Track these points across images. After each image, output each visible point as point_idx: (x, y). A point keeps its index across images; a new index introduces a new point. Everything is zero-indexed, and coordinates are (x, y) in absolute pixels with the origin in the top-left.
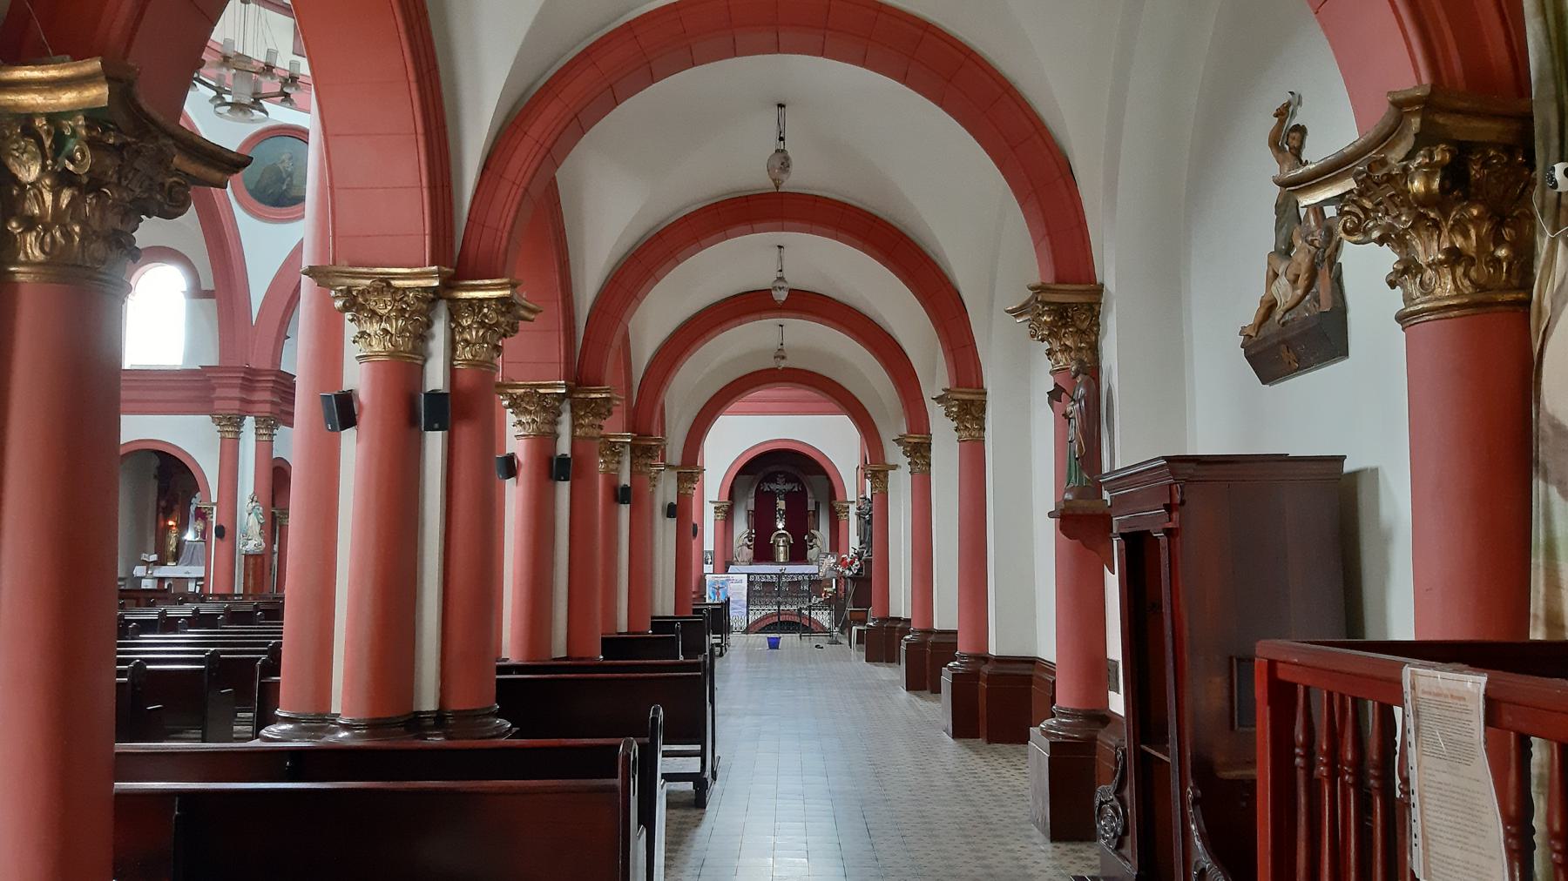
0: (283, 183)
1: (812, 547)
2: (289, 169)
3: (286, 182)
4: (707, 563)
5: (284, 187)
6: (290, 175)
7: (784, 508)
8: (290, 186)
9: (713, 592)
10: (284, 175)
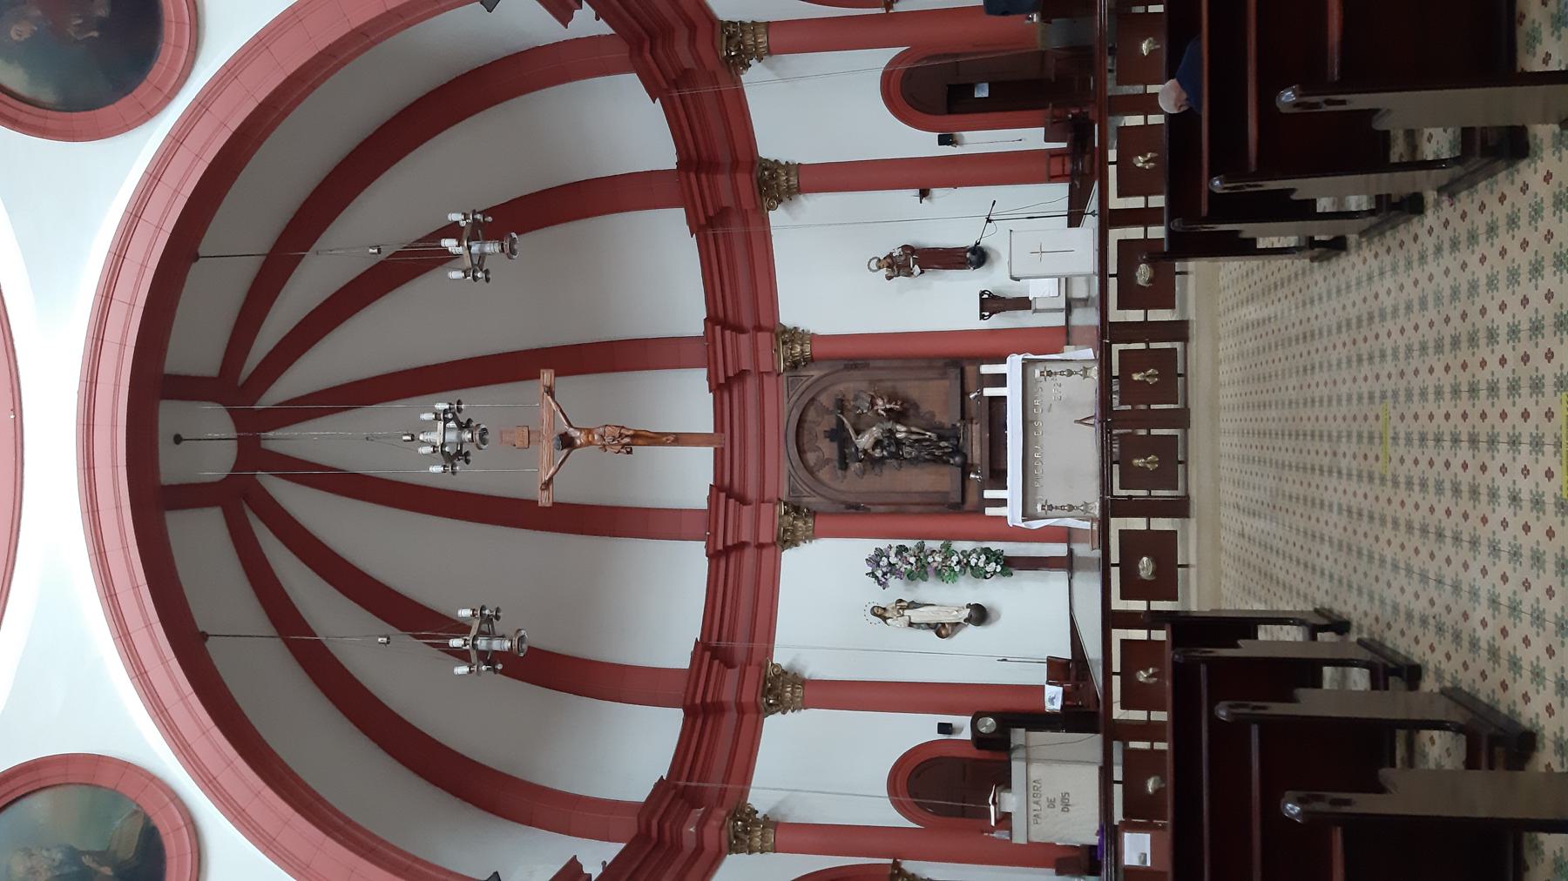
0: (96, 873)
2: (59, 856)
3: (94, 865)
5: (107, 871)
6: (74, 855)
8: (101, 856)
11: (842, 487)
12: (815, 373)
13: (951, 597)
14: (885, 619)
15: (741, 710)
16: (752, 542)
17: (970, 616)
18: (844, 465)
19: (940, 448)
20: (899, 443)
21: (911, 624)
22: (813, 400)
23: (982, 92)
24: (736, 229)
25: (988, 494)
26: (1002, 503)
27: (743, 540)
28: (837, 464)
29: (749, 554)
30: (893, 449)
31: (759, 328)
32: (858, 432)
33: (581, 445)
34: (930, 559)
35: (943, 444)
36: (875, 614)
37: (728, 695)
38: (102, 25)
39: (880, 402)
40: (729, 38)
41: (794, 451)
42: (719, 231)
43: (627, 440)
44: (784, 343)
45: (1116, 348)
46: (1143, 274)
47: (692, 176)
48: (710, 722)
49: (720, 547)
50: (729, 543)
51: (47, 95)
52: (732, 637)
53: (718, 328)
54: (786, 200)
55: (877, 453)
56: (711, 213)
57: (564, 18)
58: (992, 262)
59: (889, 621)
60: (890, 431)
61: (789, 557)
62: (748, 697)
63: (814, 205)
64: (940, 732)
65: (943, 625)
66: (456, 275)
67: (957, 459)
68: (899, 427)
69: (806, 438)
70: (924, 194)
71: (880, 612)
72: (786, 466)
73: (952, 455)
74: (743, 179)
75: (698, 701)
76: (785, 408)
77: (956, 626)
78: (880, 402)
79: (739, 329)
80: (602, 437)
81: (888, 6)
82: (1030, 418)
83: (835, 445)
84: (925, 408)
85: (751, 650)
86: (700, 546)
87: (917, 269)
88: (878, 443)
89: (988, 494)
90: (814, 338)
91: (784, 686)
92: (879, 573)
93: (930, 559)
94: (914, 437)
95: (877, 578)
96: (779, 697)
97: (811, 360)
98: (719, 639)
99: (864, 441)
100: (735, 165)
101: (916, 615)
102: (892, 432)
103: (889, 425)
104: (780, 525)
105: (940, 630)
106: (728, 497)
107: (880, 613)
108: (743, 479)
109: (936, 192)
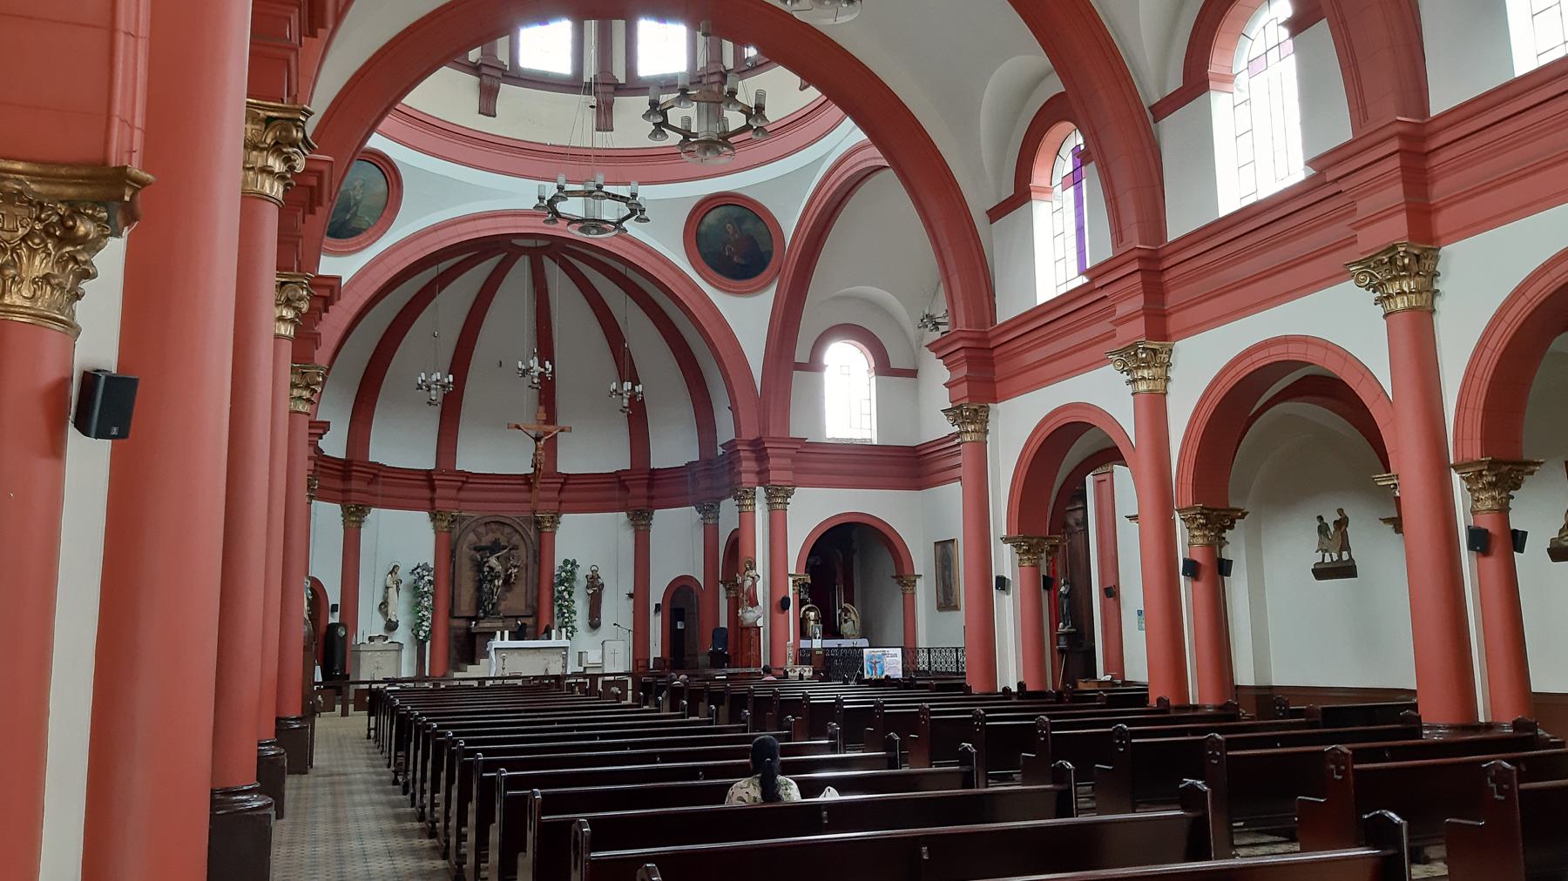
0: (348, 212)
1: (846, 621)
2: (358, 198)
3: (351, 212)
4: (816, 638)
6: (357, 204)
7: (810, 582)
8: (355, 214)
9: (871, 667)
10: (352, 204)
11: (464, 547)
12: (532, 533)
13: (400, 608)
14: (391, 573)
15: (343, 491)
16: (436, 496)
17: (392, 622)
18: (478, 549)
19: (489, 604)
20: (491, 581)
21: (387, 588)
22: (517, 531)
23: (680, 626)
24: (617, 494)
25: (507, 633)
26: (502, 639)
27: (438, 490)
28: (478, 545)
29: (427, 493)
30: (489, 578)
31: (560, 502)
32: (498, 557)
33: (536, 445)
34: (426, 599)
35: (490, 606)
36: (394, 567)
37: (355, 485)
38: (730, 258)
39: (516, 570)
40: (712, 506)
41: (488, 520)
42: (617, 485)
43: (538, 466)
44: (552, 517)
45: (588, 680)
46: (615, 689)
47: (647, 476)
48: (338, 473)
49: (434, 477)
50: (436, 482)
51: (703, 228)
52: (384, 484)
53: (562, 480)
54: (632, 523)
55: (486, 569)
56: (627, 483)
57: (722, 446)
58: (590, 632)
59: (390, 575)
60: (500, 576)
61: (425, 515)
62: (354, 495)
63: (627, 538)
64: (333, 605)
65: (387, 607)
66: (614, 386)
67: (482, 615)
68: (501, 582)
69: (493, 526)
70: (631, 596)
71: (395, 570)
72: (476, 515)
73: (485, 611)
74: (645, 501)
75: (354, 468)
76: (511, 515)
77: (385, 614)
78: (516, 570)
79: (561, 491)
80: (540, 455)
81: (721, 582)
82: (541, 650)
83: (489, 544)
84: (508, 595)
85: (376, 495)
86: (432, 467)
87: (591, 592)
88: (492, 569)
89: (507, 633)
90: (553, 533)
91: (357, 516)
92: (419, 570)
93: (426, 599)
94: (495, 590)
95: (417, 568)
96: (352, 514)
97: (540, 532)
98: (384, 477)
99: (493, 561)
100: (651, 498)
101: (392, 591)
102: (498, 577)
103: (502, 576)
104: (445, 512)
105: (384, 606)
106: (463, 482)
107: (394, 571)
108: (471, 490)
109: (632, 601)
